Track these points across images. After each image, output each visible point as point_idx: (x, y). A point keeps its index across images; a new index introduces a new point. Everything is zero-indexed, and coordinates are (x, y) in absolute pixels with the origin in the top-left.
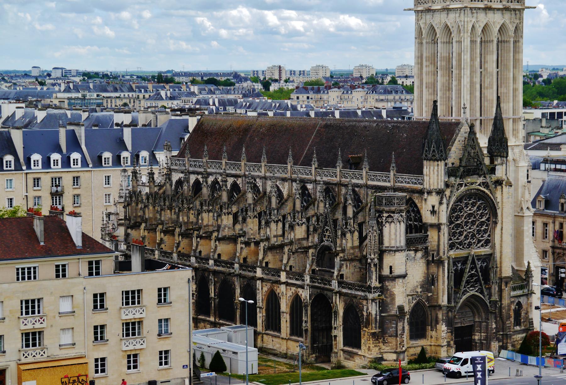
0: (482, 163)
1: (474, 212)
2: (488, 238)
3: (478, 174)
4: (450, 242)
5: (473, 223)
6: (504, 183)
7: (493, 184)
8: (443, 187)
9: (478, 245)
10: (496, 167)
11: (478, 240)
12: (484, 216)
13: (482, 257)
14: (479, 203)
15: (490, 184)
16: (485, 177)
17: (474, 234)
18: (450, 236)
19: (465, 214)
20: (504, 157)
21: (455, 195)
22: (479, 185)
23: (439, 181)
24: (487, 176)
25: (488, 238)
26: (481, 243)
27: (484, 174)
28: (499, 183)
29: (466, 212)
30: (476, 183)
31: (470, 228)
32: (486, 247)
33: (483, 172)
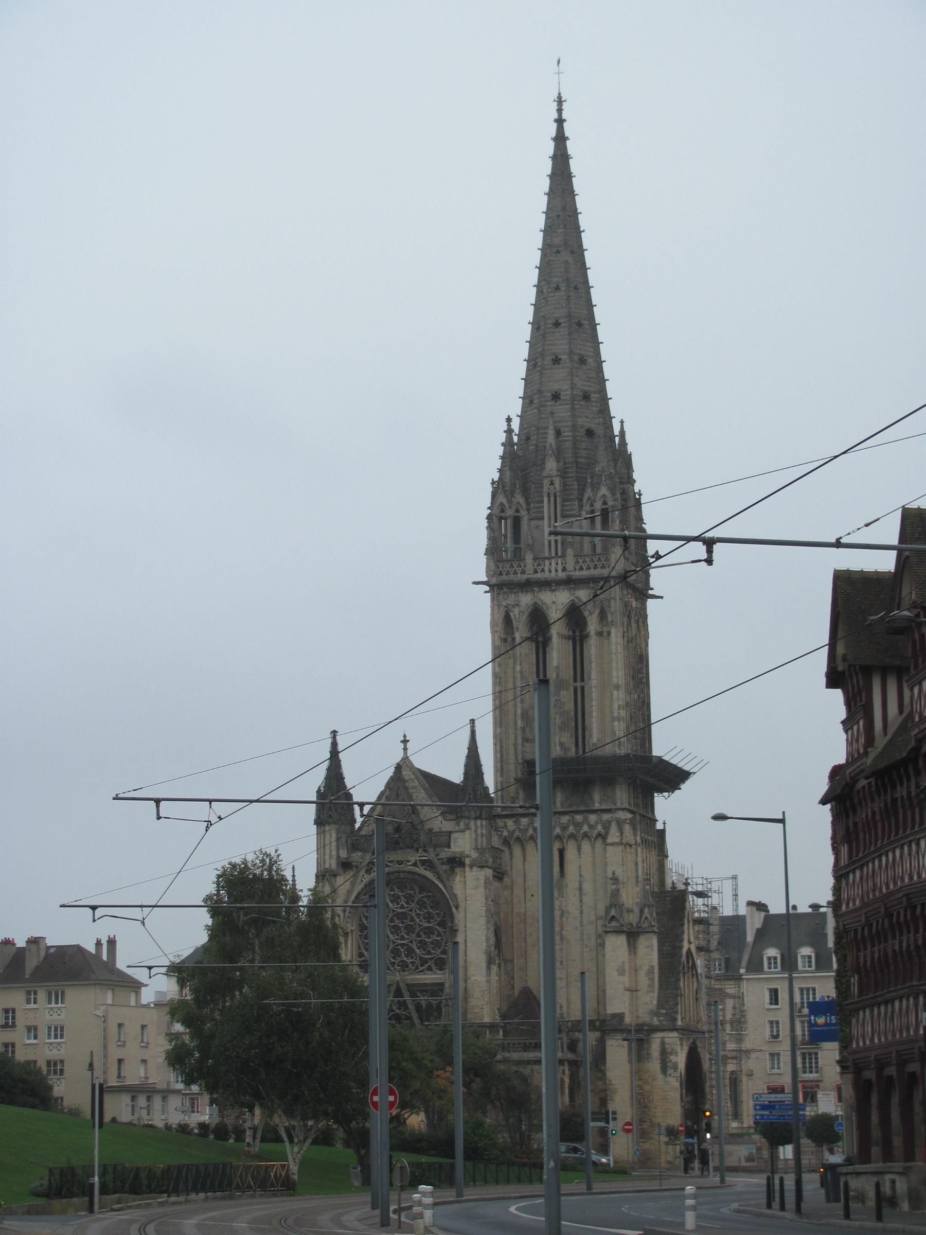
0: (419, 827)
1: (411, 910)
2: (442, 956)
3: (412, 847)
4: (361, 960)
5: (410, 929)
6: (467, 861)
7: (442, 864)
8: (334, 867)
9: (422, 968)
10: (452, 836)
11: (421, 958)
12: (433, 918)
13: (429, 988)
14: (421, 896)
15: (437, 862)
16: (425, 851)
17: (411, 948)
18: (359, 948)
19: (390, 916)
20: (469, 818)
21: (362, 881)
22: (415, 865)
23: (327, 857)
24: (431, 850)
25: (442, 956)
26: (428, 965)
27: (425, 847)
28: (456, 862)
29: (393, 911)
30: (408, 861)
31: (403, 938)
32: (440, 972)
33: (422, 845)
